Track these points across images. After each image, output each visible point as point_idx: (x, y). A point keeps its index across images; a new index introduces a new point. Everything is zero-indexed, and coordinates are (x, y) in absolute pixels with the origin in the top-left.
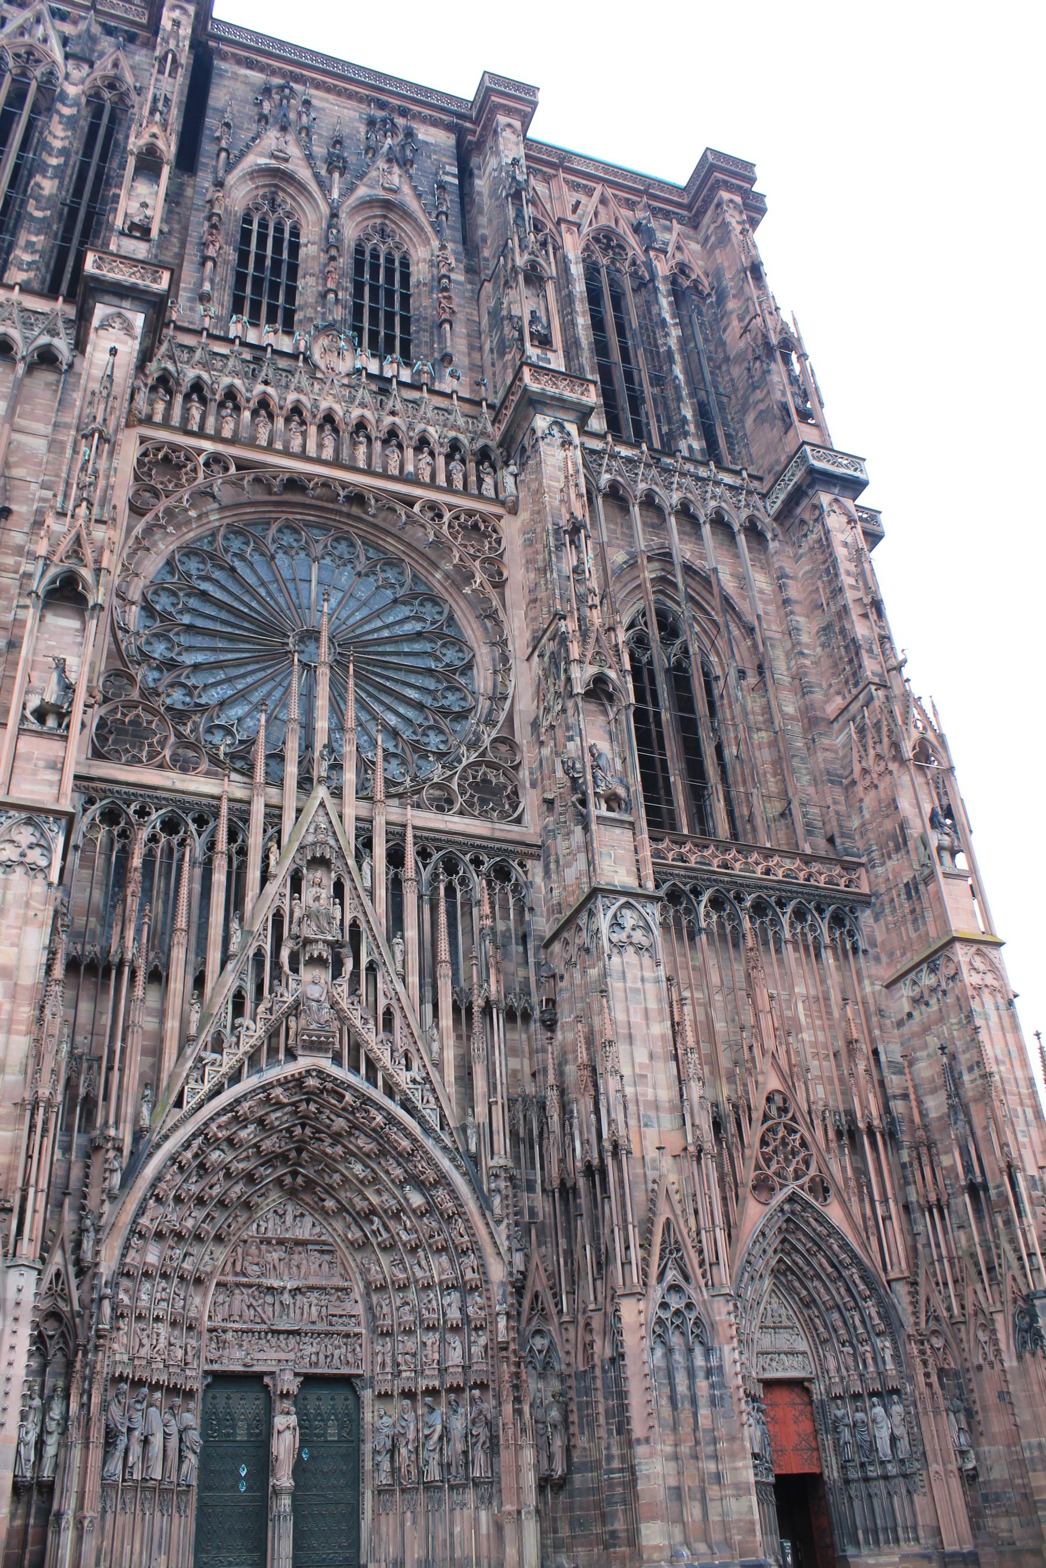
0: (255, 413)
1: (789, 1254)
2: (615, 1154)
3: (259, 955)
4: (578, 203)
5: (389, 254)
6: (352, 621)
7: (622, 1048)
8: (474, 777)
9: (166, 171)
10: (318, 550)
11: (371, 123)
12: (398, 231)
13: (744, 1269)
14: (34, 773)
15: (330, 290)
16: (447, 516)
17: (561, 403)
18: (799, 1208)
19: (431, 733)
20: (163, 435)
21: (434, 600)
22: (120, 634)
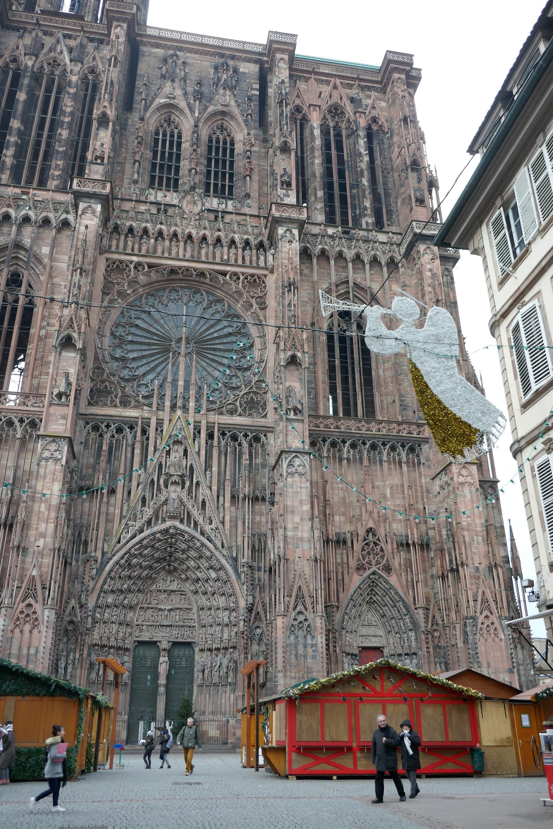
0: (156, 239)
1: (374, 595)
5: (225, 139)
6: (201, 330)
8: (247, 399)
9: (111, 124)
11: (216, 68)
12: (229, 126)
13: (349, 602)
15: (193, 168)
17: (290, 220)
18: (377, 577)
20: (116, 256)
21: (238, 316)
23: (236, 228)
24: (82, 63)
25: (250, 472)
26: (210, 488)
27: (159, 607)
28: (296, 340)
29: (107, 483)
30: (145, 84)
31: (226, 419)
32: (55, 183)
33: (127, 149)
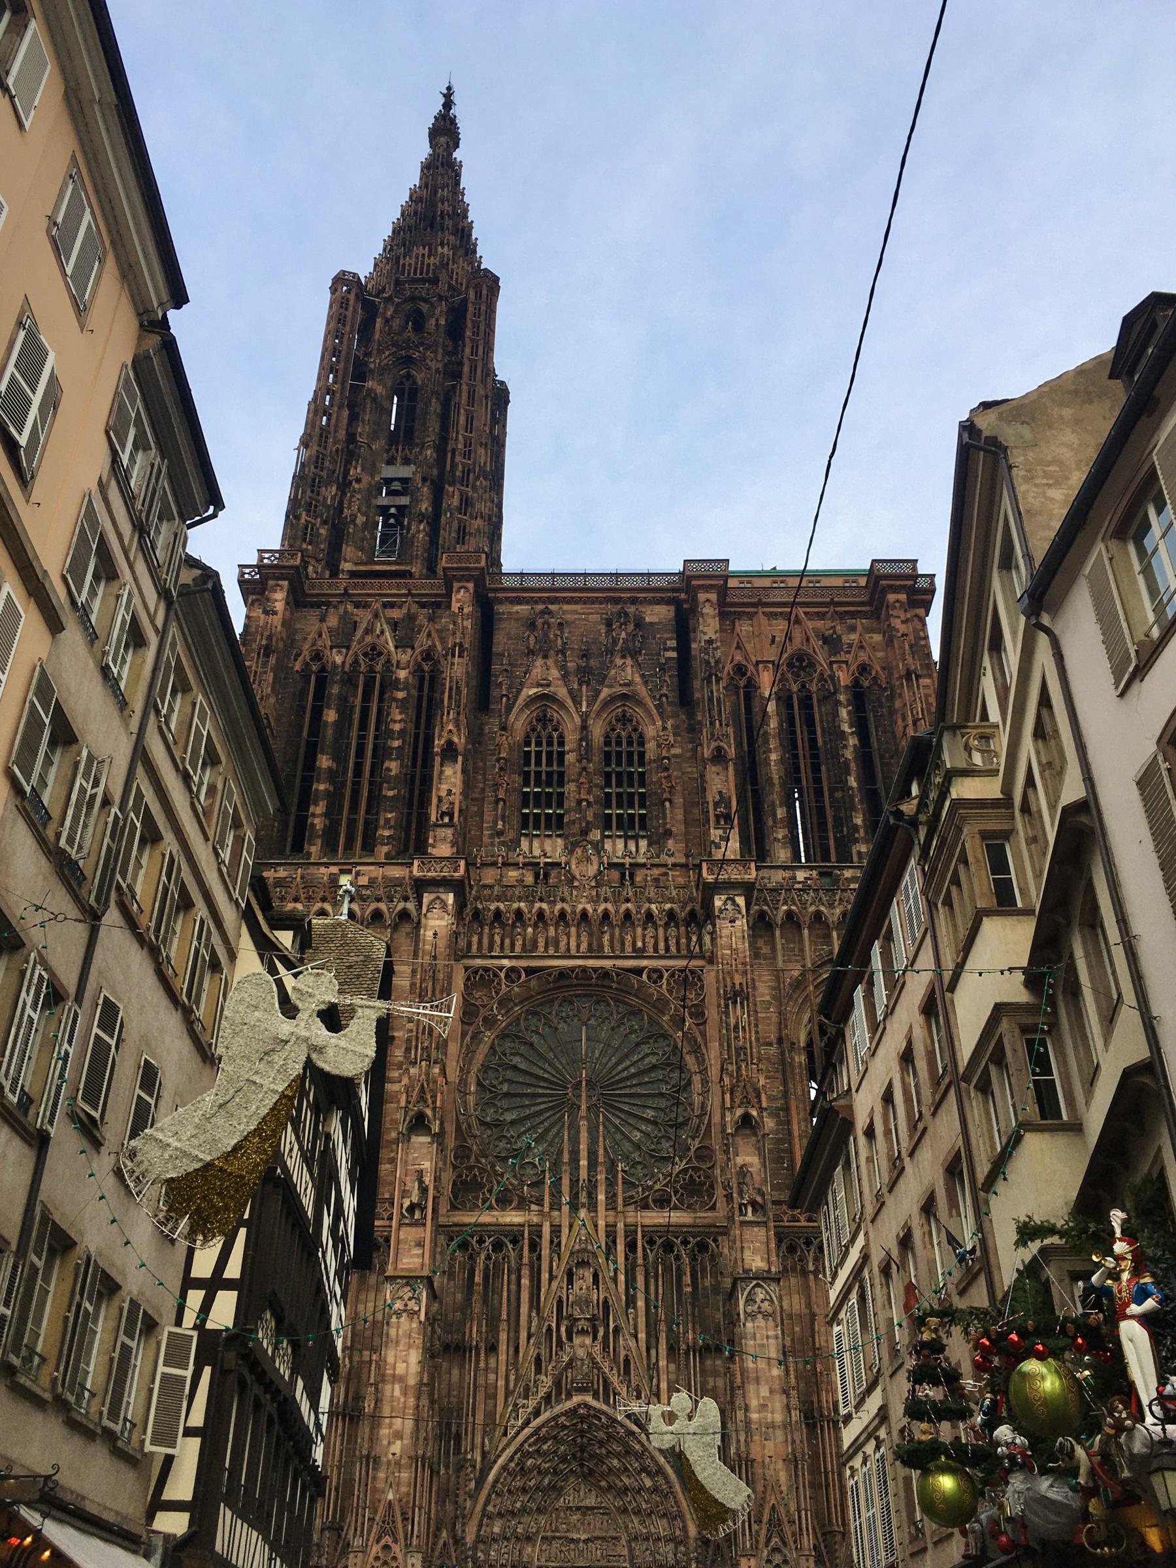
0: (535, 926)
2: (740, 1461)
3: (549, 1329)
4: (774, 637)
5: (630, 737)
6: (610, 1065)
7: (751, 1388)
9: (460, 758)
10: (585, 1015)
11: (609, 624)
14: (410, 1250)
16: (666, 975)
19: (663, 1141)
20: (479, 962)
21: (665, 1036)
22: (462, 1117)
23: (652, 894)
24: (413, 648)
25: (693, 1306)
26: (636, 1337)
27: (570, 1535)
28: (750, 1090)
29: (484, 1335)
30: (506, 670)
31: (654, 1217)
32: (385, 849)
33: (484, 775)
